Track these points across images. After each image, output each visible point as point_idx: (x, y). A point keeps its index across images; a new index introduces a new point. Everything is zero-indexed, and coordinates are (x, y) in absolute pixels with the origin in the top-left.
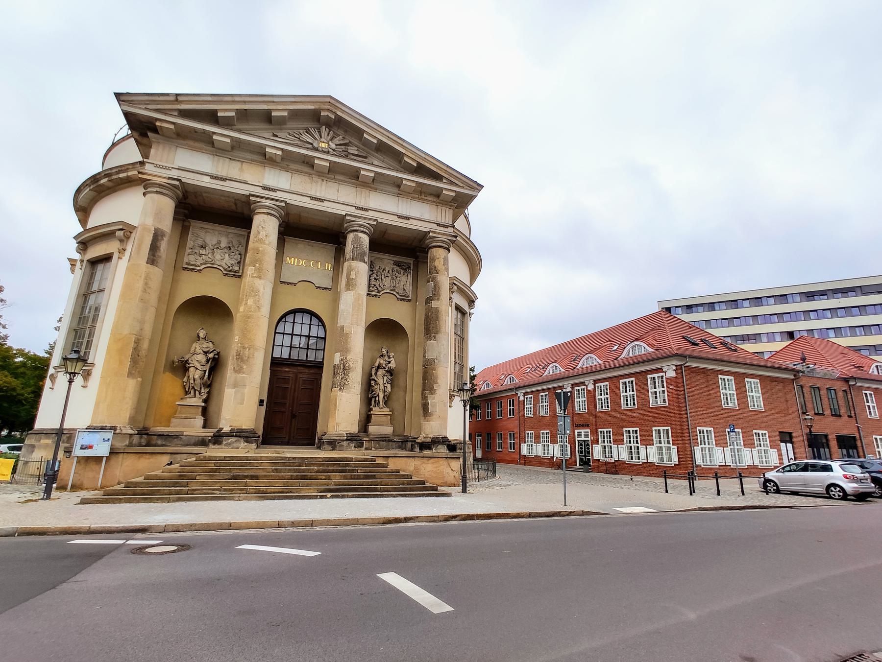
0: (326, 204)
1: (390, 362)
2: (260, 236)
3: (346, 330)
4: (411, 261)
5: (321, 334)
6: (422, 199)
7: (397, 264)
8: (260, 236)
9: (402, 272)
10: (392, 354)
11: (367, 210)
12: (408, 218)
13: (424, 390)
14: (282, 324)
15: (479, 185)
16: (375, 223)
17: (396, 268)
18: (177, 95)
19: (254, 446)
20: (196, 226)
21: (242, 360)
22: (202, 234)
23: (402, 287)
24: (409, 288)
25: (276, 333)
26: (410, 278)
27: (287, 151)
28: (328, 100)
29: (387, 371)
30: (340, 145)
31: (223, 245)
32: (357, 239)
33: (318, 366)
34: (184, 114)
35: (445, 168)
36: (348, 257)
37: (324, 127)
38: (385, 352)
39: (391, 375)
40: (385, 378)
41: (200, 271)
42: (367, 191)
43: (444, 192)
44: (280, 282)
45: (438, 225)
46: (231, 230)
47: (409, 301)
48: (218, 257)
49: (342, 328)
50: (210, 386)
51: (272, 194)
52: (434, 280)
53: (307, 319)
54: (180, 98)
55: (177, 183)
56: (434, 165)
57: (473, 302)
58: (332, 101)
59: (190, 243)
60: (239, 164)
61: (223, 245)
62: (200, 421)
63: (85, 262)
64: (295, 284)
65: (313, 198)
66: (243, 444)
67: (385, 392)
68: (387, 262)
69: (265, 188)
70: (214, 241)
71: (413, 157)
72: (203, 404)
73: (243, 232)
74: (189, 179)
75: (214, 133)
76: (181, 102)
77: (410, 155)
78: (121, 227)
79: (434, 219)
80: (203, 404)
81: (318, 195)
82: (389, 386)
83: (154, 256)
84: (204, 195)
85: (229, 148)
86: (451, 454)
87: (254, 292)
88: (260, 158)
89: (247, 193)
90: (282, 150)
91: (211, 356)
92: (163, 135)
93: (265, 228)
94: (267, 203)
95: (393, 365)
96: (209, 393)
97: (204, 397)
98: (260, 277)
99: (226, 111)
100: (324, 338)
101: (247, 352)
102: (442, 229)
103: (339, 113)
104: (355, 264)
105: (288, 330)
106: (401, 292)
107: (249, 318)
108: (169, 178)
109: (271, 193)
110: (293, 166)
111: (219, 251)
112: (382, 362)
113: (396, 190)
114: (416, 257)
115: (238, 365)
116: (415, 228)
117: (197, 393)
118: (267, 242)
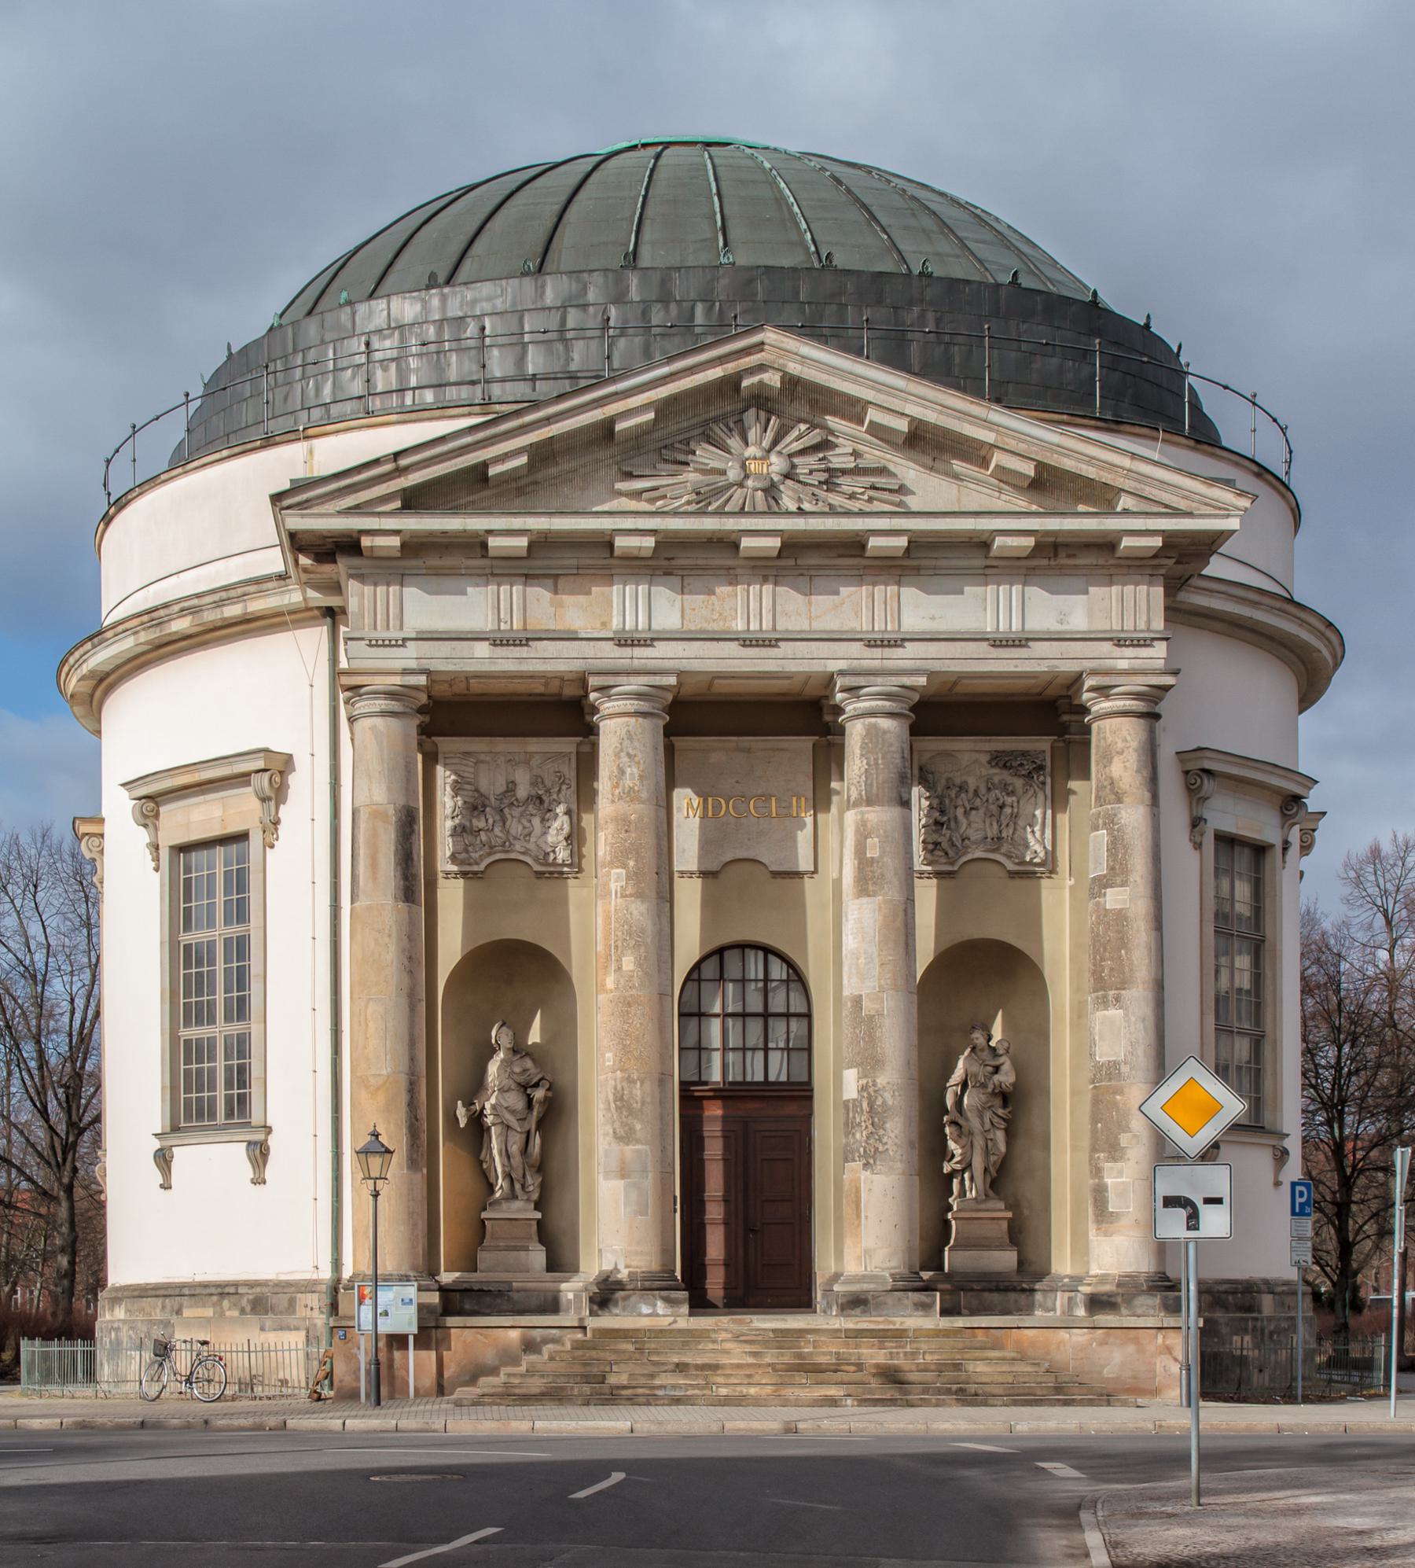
5: (797, 1006)
6: (1061, 567)
7: (999, 760)
9: (1019, 783)
11: (897, 643)
12: (1020, 642)
13: (1094, 1149)
16: (922, 681)
17: (999, 775)
19: (685, 1309)
27: (667, 532)
29: (993, 1094)
30: (802, 452)
31: (522, 792)
33: (798, 1095)
34: (412, 501)
37: (752, 412)
39: (1005, 1105)
40: (988, 1115)
45: (1120, 643)
46: (536, 745)
48: (516, 828)
50: (541, 1168)
51: (641, 655)
55: (422, 680)
57: (1296, 799)
61: (522, 792)
62: (538, 1257)
63: (164, 854)
66: (661, 1307)
67: (987, 1152)
68: (969, 755)
69: (625, 641)
70: (501, 787)
71: (1022, 447)
72: (539, 1215)
73: (567, 745)
74: (447, 659)
75: (490, 532)
77: (1012, 444)
78: (260, 764)
79: (1101, 625)
80: (539, 1215)
82: (1000, 1136)
86: (1170, 1321)
89: (577, 666)
91: (539, 1094)
95: (1006, 1077)
96: (543, 1186)
97: (535, 1196)
99: (506, 456)
100: (808, 1016)
102: (1129, 652)
103: (794, 368)
108: (406, 672)
109: (638, 652)
111: (516, 812)
114: (1062, 730)
115: (623, 1124)
116: (1043, 667)
117: (518, 1186)
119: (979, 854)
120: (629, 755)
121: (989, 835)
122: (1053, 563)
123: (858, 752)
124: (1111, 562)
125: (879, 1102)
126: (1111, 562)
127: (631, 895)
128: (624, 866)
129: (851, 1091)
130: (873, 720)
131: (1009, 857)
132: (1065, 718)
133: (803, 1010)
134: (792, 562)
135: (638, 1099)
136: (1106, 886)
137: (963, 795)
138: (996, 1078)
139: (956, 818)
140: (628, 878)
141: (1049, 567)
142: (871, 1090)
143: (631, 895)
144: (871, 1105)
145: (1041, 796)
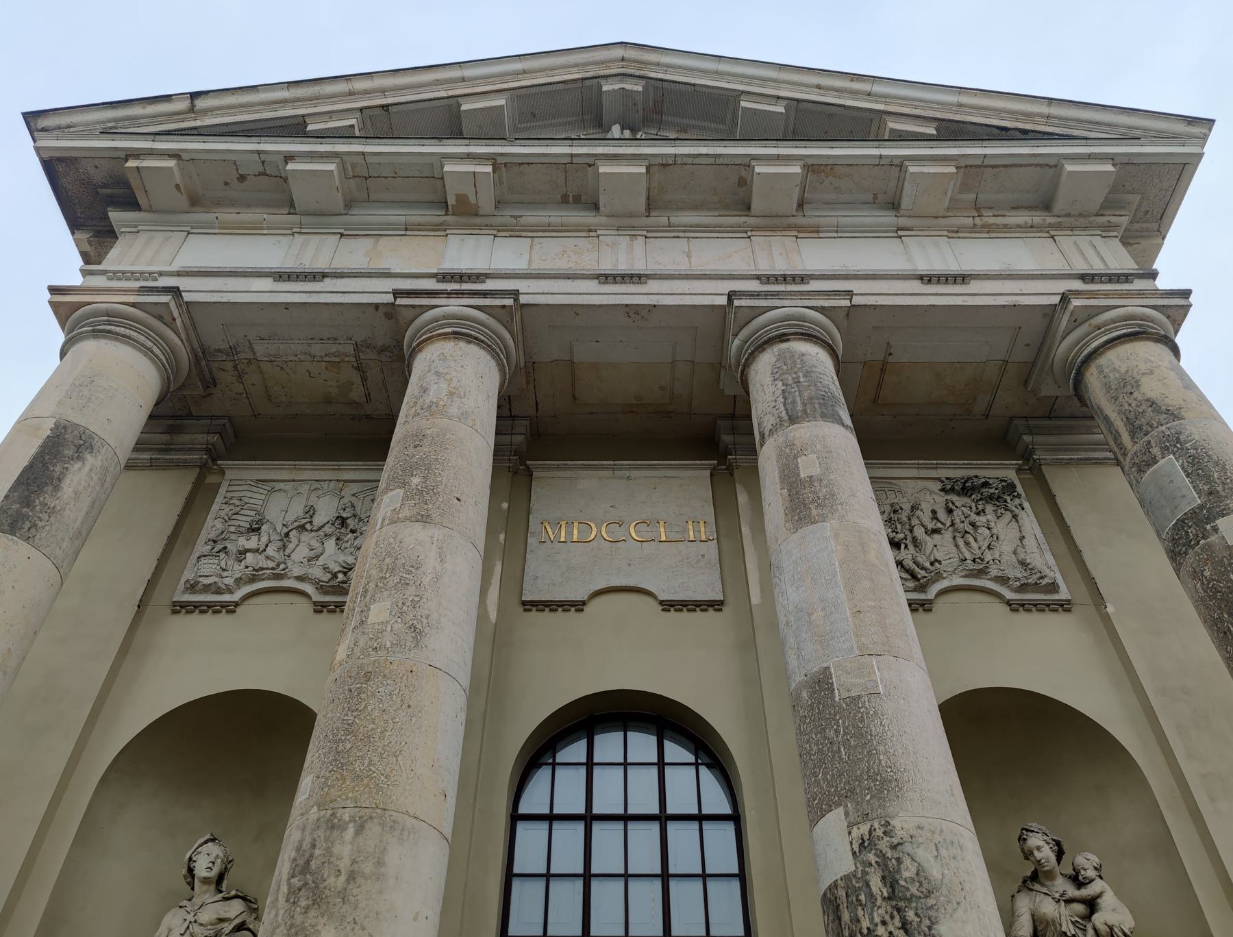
0: (653, 286)
1: (1092, 905)
2: (431, 397)
3: (844, 684)
4: (1008, 472)
8: (431, 397)
10: (1087, 862)
14: (542, 777)
15: (1191, 121)
18: (194, 95)
20: (242, 482)
21: (318, 899)
22: (256, 497)
23: (1008, 558)
24: (1045, 561)
25: (516, 818)
26: (1028, 520)
28: (618, 53)
32: (789, 370)
35: (1044, 109)
36: (769, 421)
38: (1046, 853)
41: (230, 608)
42: (789, 242)
43: (1069, 168)
44: (520, 607)
47: (1064, 606)
49: (821, 683)
52: (1174, 444)
53: (643, 745)
54: (201, 104)
56: (1000, 112)
58: (631, 54)
59: (212, 525)
60: (368, 242)
64: (579, 606)
65: (605, 278)
75: (289, 157)
76: (205, 112)
81: (623, 267)
83: (28, 503)
84: (261, 349)
85: (340, 207)
87: (402, 573)
88: (433, 216)
90: (492, 159)
92: (150, 210)
93: (455, 396)
94: (453, 306)
98: (424, 519)
100: (735, 817)
101: (344, 849)
104: (803, 432)
105: (570, 800)
106: (1018, 573)
107: (368, 677)
110: (531, 217)
112: (1048, 908)
113: (888, 218)
118: (454, 410)
119: (958, 581)
120: (437, 373)
121: (968, 555)
122: (977, 220)
123: (769, 380)
124: (1050, 220)
125: (908, 871)
126: (1050, 220)
127: (409, 519)
128: (404, 484)
129: (837, 859)
130: (785, 345)
131: (1003, 580)
132: (1027, 438)
133: (727, 809)
134: (664, 220)
135: (344, 865)
136: (1211, 518)
137: (918, 513)
138: (1098, 919)
139: (914, 540)
140: (406, 497)
141: (974, 229)
142: (883, 845)
143: (409, 519)
144: (890, 880)
145: (1022, 514)
